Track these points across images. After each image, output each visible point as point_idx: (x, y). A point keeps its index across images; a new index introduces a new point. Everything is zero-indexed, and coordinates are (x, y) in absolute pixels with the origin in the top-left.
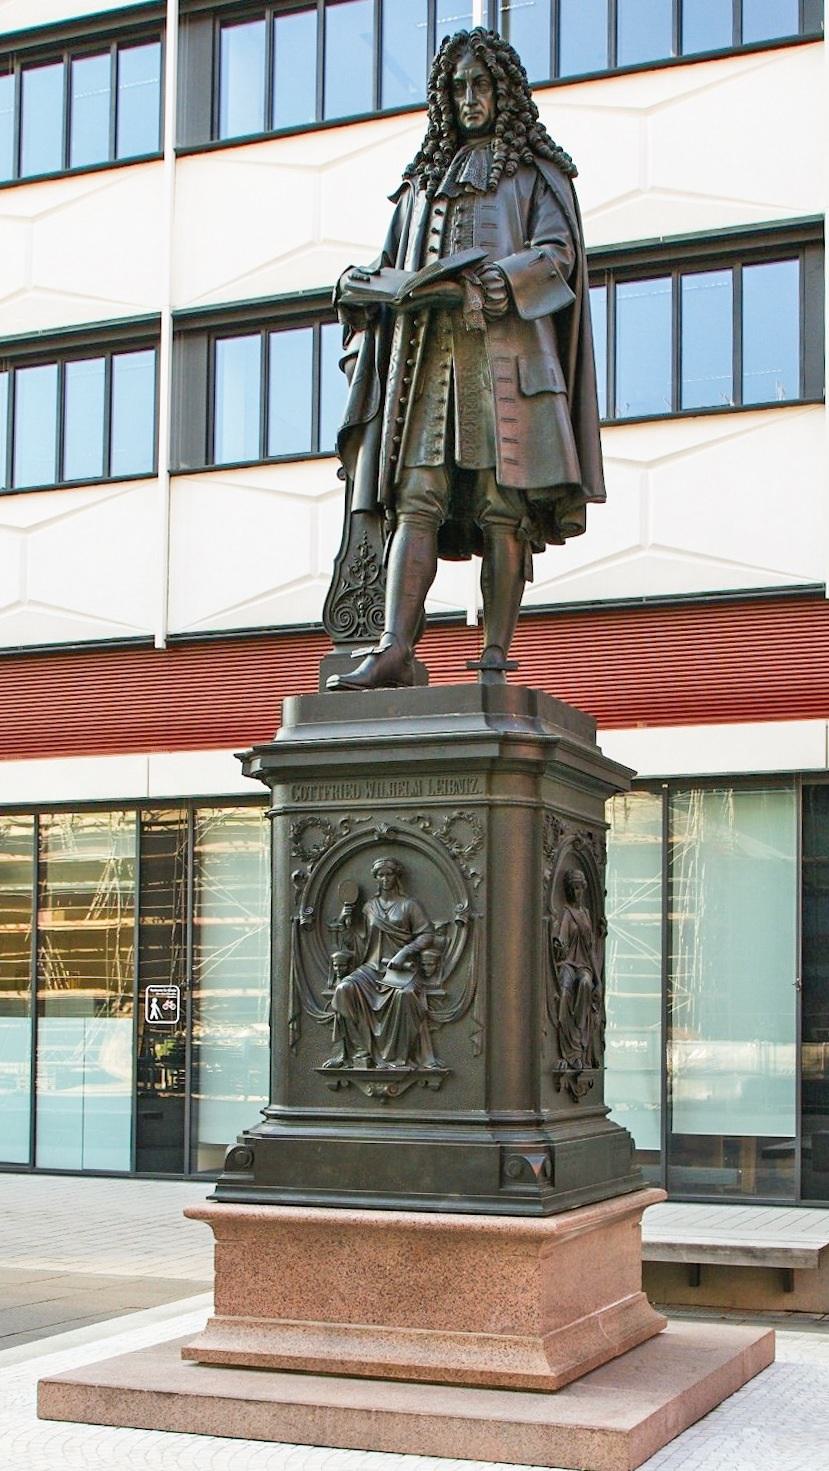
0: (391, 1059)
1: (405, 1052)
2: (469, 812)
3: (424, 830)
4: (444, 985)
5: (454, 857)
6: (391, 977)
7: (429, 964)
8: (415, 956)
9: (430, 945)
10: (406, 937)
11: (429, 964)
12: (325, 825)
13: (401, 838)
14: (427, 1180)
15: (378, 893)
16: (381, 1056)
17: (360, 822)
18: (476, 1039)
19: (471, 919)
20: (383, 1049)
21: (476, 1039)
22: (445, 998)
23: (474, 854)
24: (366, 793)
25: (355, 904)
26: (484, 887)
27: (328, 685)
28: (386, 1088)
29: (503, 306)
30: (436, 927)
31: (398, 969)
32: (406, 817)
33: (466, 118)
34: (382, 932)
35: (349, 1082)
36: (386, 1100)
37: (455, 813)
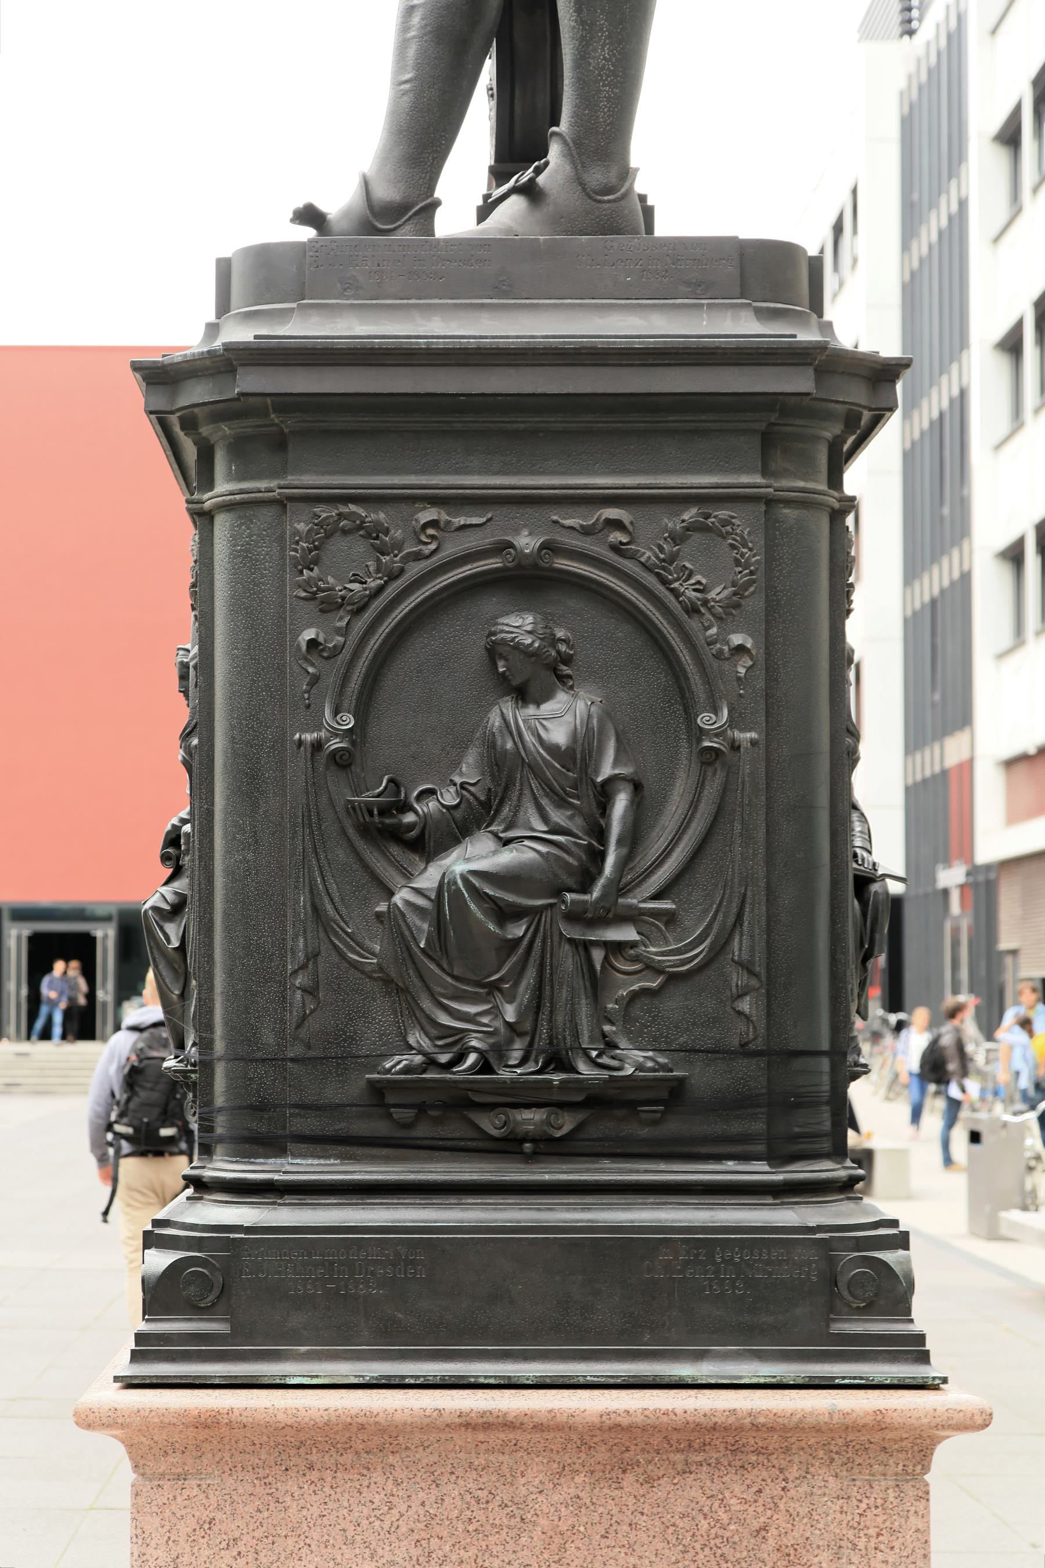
2: (723, 513)
5: (692, 610)
13: (563, 564)
18: (745, 1005)
19: (735, 747)
21: (745, 1005)
23: (737, 606)
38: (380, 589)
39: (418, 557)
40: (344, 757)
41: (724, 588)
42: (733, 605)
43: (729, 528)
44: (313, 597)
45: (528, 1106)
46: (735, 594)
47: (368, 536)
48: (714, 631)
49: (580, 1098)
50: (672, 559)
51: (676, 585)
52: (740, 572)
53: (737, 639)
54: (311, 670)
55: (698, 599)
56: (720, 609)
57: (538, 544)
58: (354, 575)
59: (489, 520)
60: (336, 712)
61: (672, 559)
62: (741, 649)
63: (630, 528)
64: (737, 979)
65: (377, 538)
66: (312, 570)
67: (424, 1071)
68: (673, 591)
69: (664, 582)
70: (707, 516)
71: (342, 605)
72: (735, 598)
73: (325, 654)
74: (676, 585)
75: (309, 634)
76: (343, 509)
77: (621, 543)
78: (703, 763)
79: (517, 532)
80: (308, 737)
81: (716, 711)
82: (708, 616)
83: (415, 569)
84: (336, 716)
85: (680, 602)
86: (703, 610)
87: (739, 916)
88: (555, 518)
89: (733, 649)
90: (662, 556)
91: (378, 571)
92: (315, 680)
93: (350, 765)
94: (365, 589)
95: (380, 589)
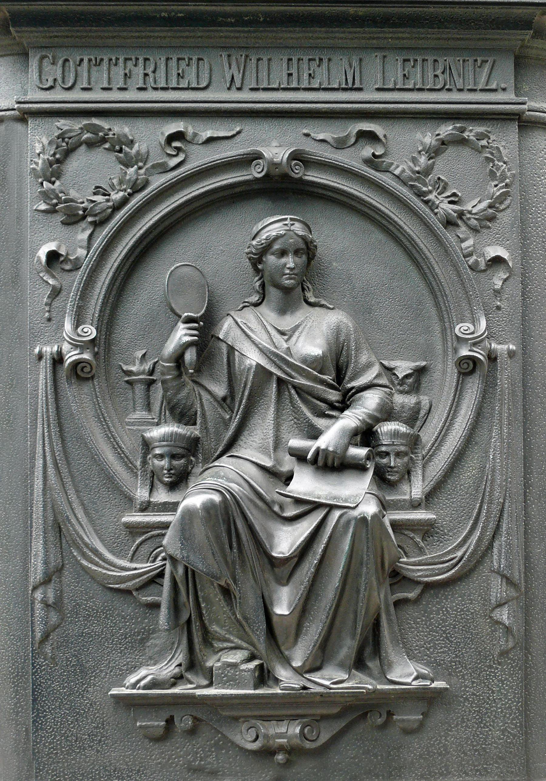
0: (314, 666)
1: (347, 648)
3: (372, 162)
4: (429, 498)
5: (449, 223)
7: (398, 454)
8: (366, 435)
9: (387, 413)
10: (334, 396)
11: (398, 454)
15: (255, 298)
16: (287, 661)
17: (211, 140)
19: (492, 358)
22: (427, 530)
23: (492, 219)
24: (229, 79)
25: (204, 317)
28: (298, 730)
30: (401, 376)
31: (331, 465)
32: (325, 132)
34: (280, 381)
35: (195, 718)
37: (446, 129)
38: (124, 202)
39: (164, 169)
40: (85, 370)
41: (480, 202)
42: (488, 219)
43: (484, 142)
44: (52, 211)
45: (280, 719)
46: (490, 206)
47: (111, 149)
48: (470, 242)
49: (335, 710)
50: (427, 171)
51: (431, 197)
52: (496, 186)
53: (493, 251)
54: (51, 281)
55: (455, 211)
56: (475, 222)
57: (286, 156)
58: (97, 187)
59: (239, 133)
60: (78, 322)
61: (427, 171)
62: (497, 261)
63: (383, 139)
64: (498, 589)
65: (120, 151)
66: (53, 183)
67: (174, 685)
68: (426, 202)
69: (420, 194)
70: (462, 130)
71: (84, 217)
72: (491, 211)
73: (68, 267)
74: (431, 197)
76: (85, 122)
77: (373, 155)
78: (460, 373)
79: (267, 143)
80: (49, 350)
81: (474, 321)
82: (463, 228)
83: (158, 181)
84: (77, 327)
85: (436, 214)
86: (460, 222)
87: (498, 527)
88: (305, 131)
89: (489, 261)
90: (417, 169)
91: (121, 182)
92: (56, 293)
93: (92, 378)
94: (108, 201)
95: (124, 202)
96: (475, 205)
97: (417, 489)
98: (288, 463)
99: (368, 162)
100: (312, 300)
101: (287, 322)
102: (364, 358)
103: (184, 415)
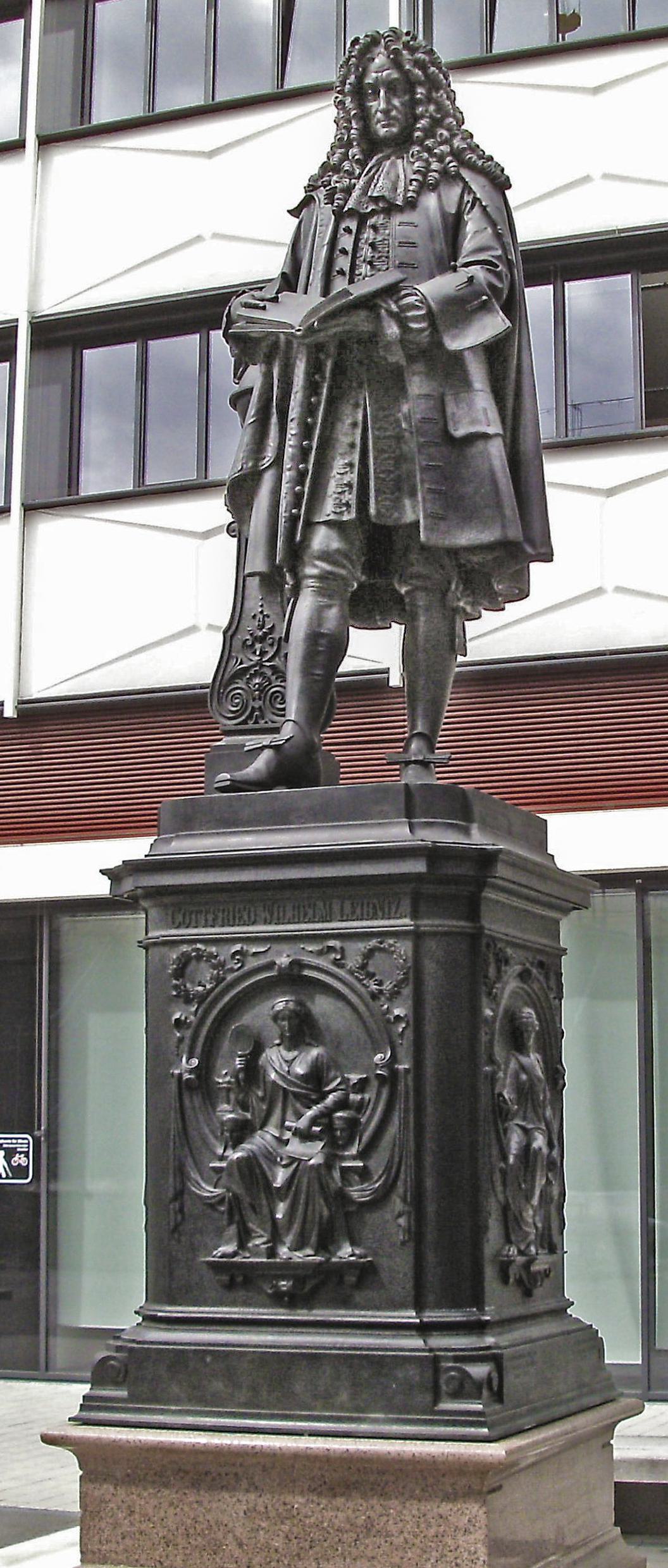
4: (361, 1155)
6: (296, 1147)
9: (342, 1104)
12: (212, 956)
14: (344, 1396)
15: (277, 1042)
20: (287, 1235)
26: (409, 1033)
27: (216, 785)
29: (424, 337)
31: (305, 1136)
33: (379, 125)
36: (291, 1300)
37: (373, 943)
38: (213, 989)
39: (232, 970)
53: (397, 1012)
62: (398, 1017)
69: (360, 981)
75: (177, 1016)
80: (177, 1072)
81: (385, 1053)
96: (387, 986)
97: (354, 1151)
98: (288, 1135)
99: (336, 963)
100: (308, 1040)
101: (290, 1055)
102: (332, 1074)
103: (245, 1107)
